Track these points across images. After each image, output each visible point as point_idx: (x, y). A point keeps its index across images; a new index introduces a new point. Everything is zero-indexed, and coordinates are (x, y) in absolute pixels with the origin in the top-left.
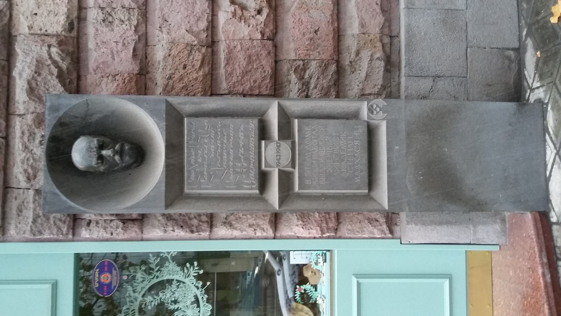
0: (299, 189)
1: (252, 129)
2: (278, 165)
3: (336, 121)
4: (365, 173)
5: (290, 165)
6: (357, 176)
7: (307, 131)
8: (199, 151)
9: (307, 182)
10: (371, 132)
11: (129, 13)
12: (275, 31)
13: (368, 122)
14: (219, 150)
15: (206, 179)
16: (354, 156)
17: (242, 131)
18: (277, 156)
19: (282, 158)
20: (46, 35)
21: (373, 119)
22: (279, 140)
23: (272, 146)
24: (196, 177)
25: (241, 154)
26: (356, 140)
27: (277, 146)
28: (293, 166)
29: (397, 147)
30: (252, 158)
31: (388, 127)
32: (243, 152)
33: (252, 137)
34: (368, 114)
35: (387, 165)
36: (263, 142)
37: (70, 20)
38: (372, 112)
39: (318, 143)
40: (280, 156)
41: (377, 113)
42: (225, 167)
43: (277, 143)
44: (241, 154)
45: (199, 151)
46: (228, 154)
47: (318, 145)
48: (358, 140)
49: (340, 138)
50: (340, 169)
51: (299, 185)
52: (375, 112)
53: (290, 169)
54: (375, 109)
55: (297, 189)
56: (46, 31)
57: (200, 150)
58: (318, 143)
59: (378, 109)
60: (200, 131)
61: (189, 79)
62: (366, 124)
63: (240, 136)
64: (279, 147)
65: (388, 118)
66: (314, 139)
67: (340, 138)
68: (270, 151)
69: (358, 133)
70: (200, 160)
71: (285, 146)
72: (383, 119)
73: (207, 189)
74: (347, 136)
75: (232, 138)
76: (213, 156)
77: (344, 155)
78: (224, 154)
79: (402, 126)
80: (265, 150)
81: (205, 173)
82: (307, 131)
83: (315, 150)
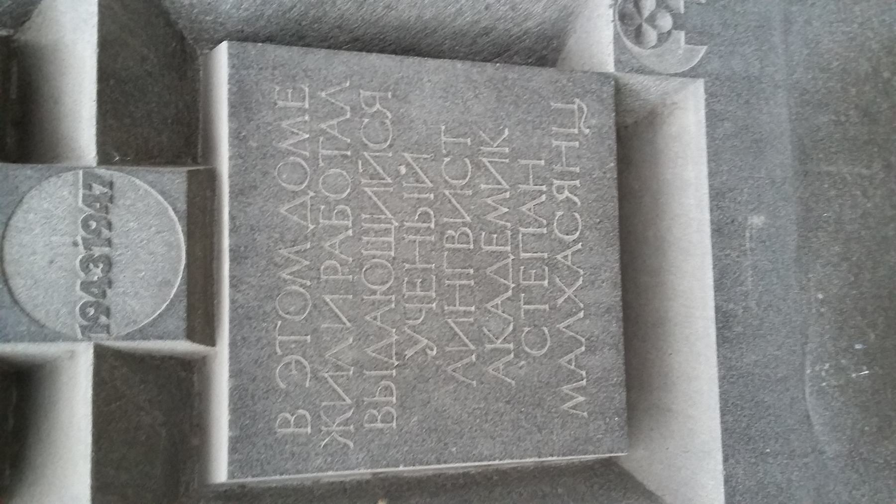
2: (96, 315)
4: (611, 359)
5: (178, 321)
6: (572, 377)
7: (286, 113)
10: (633, 138)
13: (617, 81)
16: (554, 266)
19: (123, 278)
21: (642, 70)
22: (104, 159)
26: (562, 176)
27: (89, 200)
28: (201, 325)
29: (757, 220)
31: (713, 118)
34: (617, 39)
35: (718, 309)
38: (638, 36)
39: (356, 186)
40: (109, 263)
41: (663, 38)
43: (90, 178)
47: (357, 198)
48: (573, 176)
49: (478, 166)
50: (479, 341)
51: (235, 445)
52: (651, 35)
53: (183, 346)
54: (652, 20)
55: (221, 472)
58: (356, 186)
59: (666, 22)
62: (608, 91)
64: (101, 205)
65: (715, 65)
66: (329, 159)
67: (478, 166)
69: (569, 137)
71: (149, 203)
72: (692, 74)
74: (515, 155)
77: (501, 255)
79: (777, 115)
82: (286, 113)
83: (334, 231)
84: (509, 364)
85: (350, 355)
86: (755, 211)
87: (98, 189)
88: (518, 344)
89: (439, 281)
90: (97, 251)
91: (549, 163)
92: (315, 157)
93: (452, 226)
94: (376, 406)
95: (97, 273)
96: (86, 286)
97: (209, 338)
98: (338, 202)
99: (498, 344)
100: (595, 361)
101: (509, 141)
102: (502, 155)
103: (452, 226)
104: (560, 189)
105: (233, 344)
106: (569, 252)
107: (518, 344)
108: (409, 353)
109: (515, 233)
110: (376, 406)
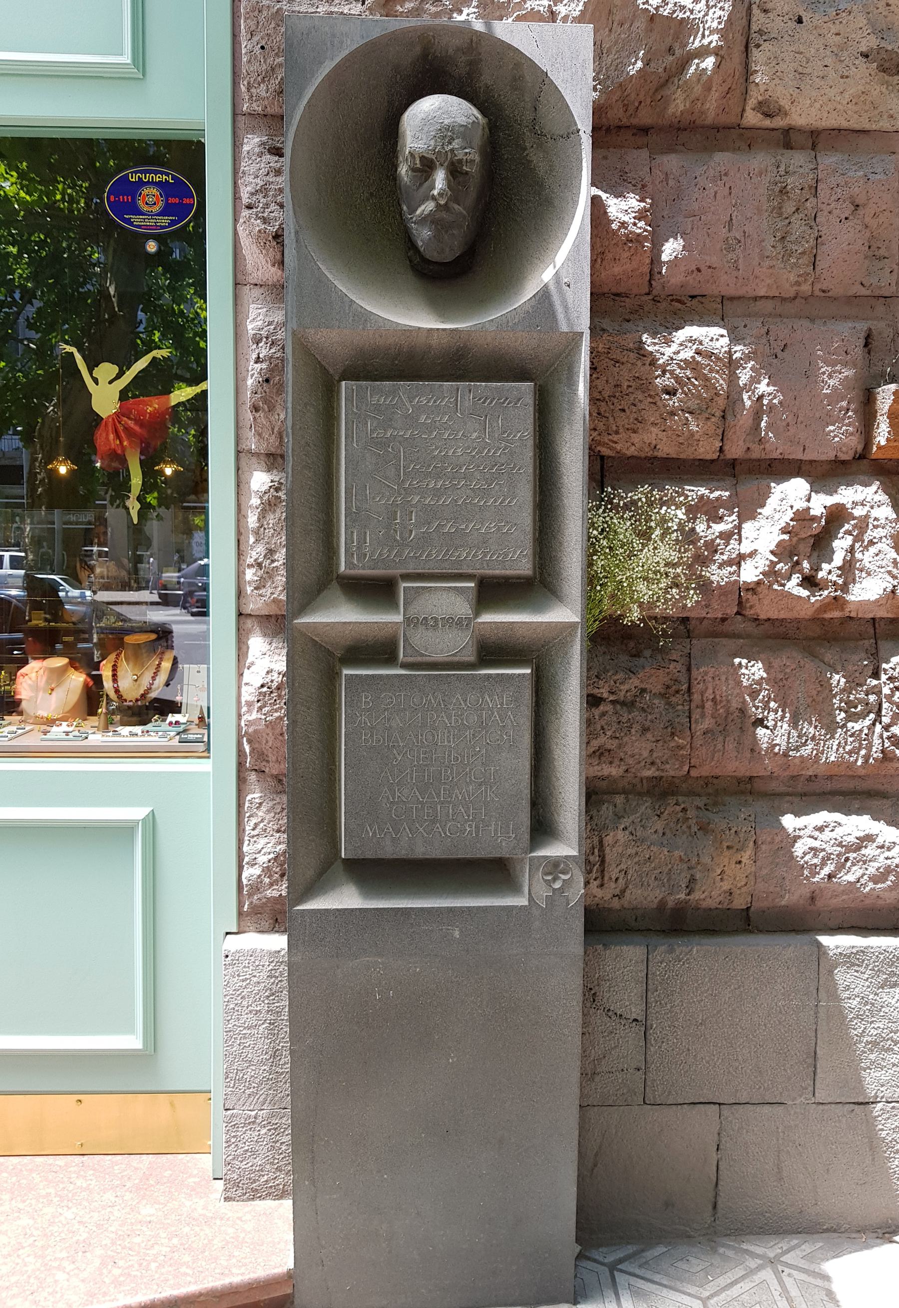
0: (349, 678)
3: (527, 777)
4: (389, 851)
6: (381, 830)
9: (366, 698)
11: (803, 253)
16: (434, 822)
17: (499, 529)
20: (747, 47)
23: (462, 607)
24: (378, 408)
29: (457, 934)
37: (785, 103)
46: (437, 493)
55: (346, 672)
56: (758, 46)
61: (640, 401)
64: (459, 623)
65: (536, 912)
68: (451, 601)
72: (531, 899)
77: (438, 795)
84: (388, 799)
85: (394, 725)
86: (461, 931)
88: (397, 803)
89: (426, 765)
91: (483, 820)
92: (484, 709)
93: (452, 773)
94: (372, 736)
97: (404, 666)
99: (397, 794)
100: (388, 842)
101: (493, 800)
102: (486, 797)
103: (452, 773)
104: (470, 826)
105: (401, 675)
106: (440, 830)
107: (397, 803)
108: (395, 752)
109: (449, 802)
110: (372, 736)
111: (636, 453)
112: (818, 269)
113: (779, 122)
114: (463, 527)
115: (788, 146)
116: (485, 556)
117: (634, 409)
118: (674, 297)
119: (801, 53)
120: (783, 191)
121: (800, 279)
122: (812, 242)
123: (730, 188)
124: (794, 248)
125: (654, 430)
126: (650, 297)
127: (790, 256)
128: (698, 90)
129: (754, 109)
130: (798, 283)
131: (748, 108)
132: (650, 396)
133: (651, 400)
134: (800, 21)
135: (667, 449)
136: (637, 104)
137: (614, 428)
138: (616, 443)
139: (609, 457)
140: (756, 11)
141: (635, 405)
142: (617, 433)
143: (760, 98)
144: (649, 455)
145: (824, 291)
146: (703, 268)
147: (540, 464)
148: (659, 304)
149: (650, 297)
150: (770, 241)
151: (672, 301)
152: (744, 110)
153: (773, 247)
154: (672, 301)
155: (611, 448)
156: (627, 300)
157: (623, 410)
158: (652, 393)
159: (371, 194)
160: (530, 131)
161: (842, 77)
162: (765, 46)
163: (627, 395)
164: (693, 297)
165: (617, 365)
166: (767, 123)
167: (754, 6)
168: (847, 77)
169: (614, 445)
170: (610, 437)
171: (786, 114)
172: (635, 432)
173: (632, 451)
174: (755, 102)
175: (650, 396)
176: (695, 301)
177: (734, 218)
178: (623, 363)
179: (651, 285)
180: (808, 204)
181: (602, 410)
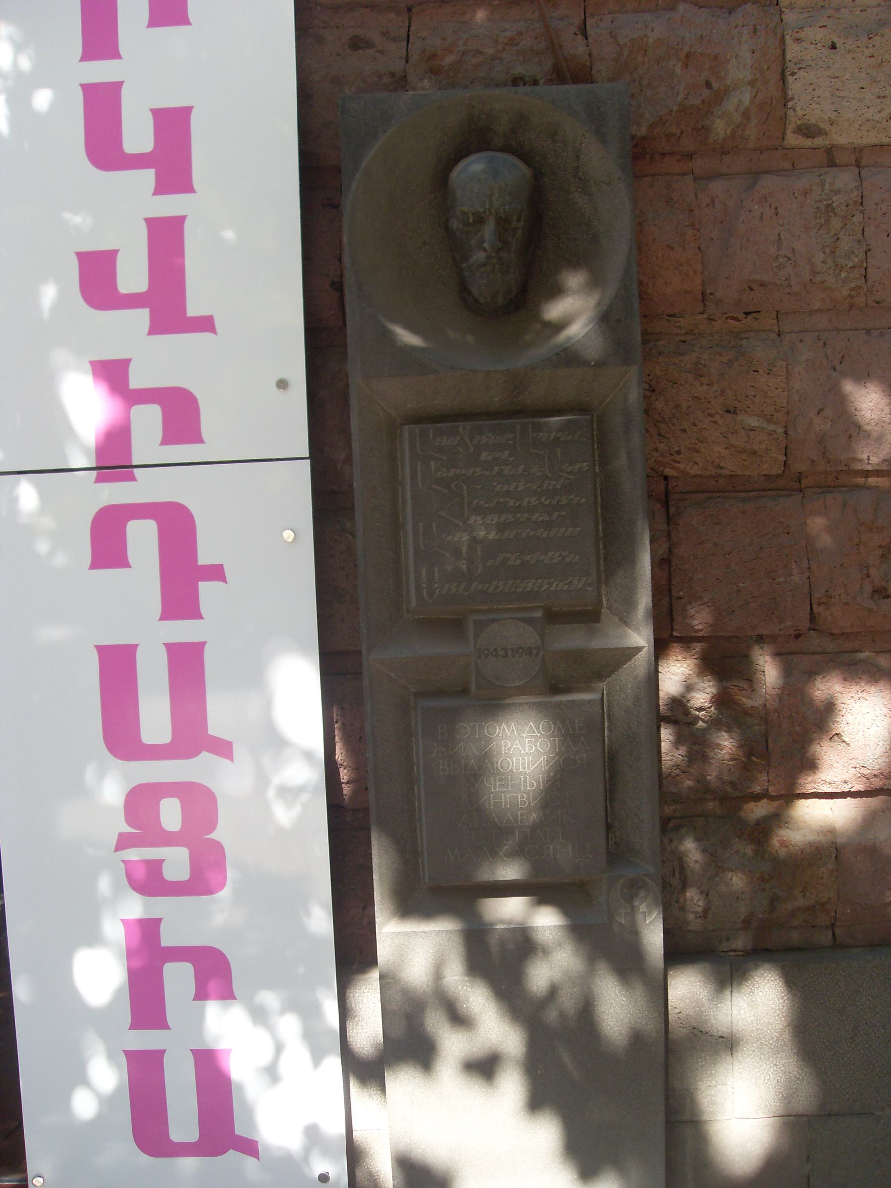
1: (570, 583)
8: (507, 453)
11: (854, 267)
12: (835, 631)
14: (511, 504)
15: (439, 475)
18: (505, 650)
20: (783, 74)
25: (506, 560)
27: (530, 649)
30: (497, 587)
32: (511, 563)
33: (551, 584)
36: (539, 614)
37: (824, 126)
42: (471, 521)
44: (506, 560)
45: (507, 453)
56: (793, 74)
57: (510, 455)
60: (559, 451)
63: (550, 554)
70: (484, 456)
73: (414, 477)
75: (545, 534)
76: (499, 488)
78: (504, 516)
80: (518, 619)
81: (453, 472)
83: (523, 747)
87: (534, 652)
90: (510, 652)
95: (502, 653)
96: (496, 650)
98: (536, 746)
111: (700, 472)
112: (870, 283)
113: (819, 141)
114: (528, 558)
115: (832, 164)
116: (551, 586)
117: (695, 429)
118: (729, 315)
119: (837, 77)
120: (829, 208)
121: (853, 293)
122: (862, 256)
123: (776, 209)
124: (844, 262)
125: (716, 449)
126: (705, 316)
127: (841, 271)
128: (737, 118)
129: (794, 132)
130: (851, 297)
131: (788, 132)
132: (710, 415)
133: (712, 419)
134: (833, 47)
135: (731, 466)
136: (678, 134)
137: (676, 449)
138: (679, 463)
139: (673, 477)
140: (788, 41)
141: (695, 425)
142: (679, 453)
143: (799, 123)
144: (713, 473)
145: (877, 303)
146: (754, 286)
147: (601, 493)
148: (713, 322)
149: (705, 316)
150: (819, 257)
151: (727, 318)
152: (784, 133)
153: (823, 262)
154: (727, 318)
155: (674, 468)
156: (682, 320)
157: (684, 431)
158: (712, 412)
159: (424, 243)
160: (574, 176)
161: (879, 97)
162: (802, 73)
163: (687, 415)
164: (747, 314)
165: (675, 386)
166: (808, 142)
167: (787, 37)
168: (884, 97)
169: (677, 465)
170: (672, 458)
171: (826, 134)
172: (697, 451)
173: (695, 470)
174: (794, 126)
175: (710, 415)
176: (750, 317)
177: (782, 237)
178: (681, 385)
179: (705, 305)
180: (855, 219)
181: (663, 432)
